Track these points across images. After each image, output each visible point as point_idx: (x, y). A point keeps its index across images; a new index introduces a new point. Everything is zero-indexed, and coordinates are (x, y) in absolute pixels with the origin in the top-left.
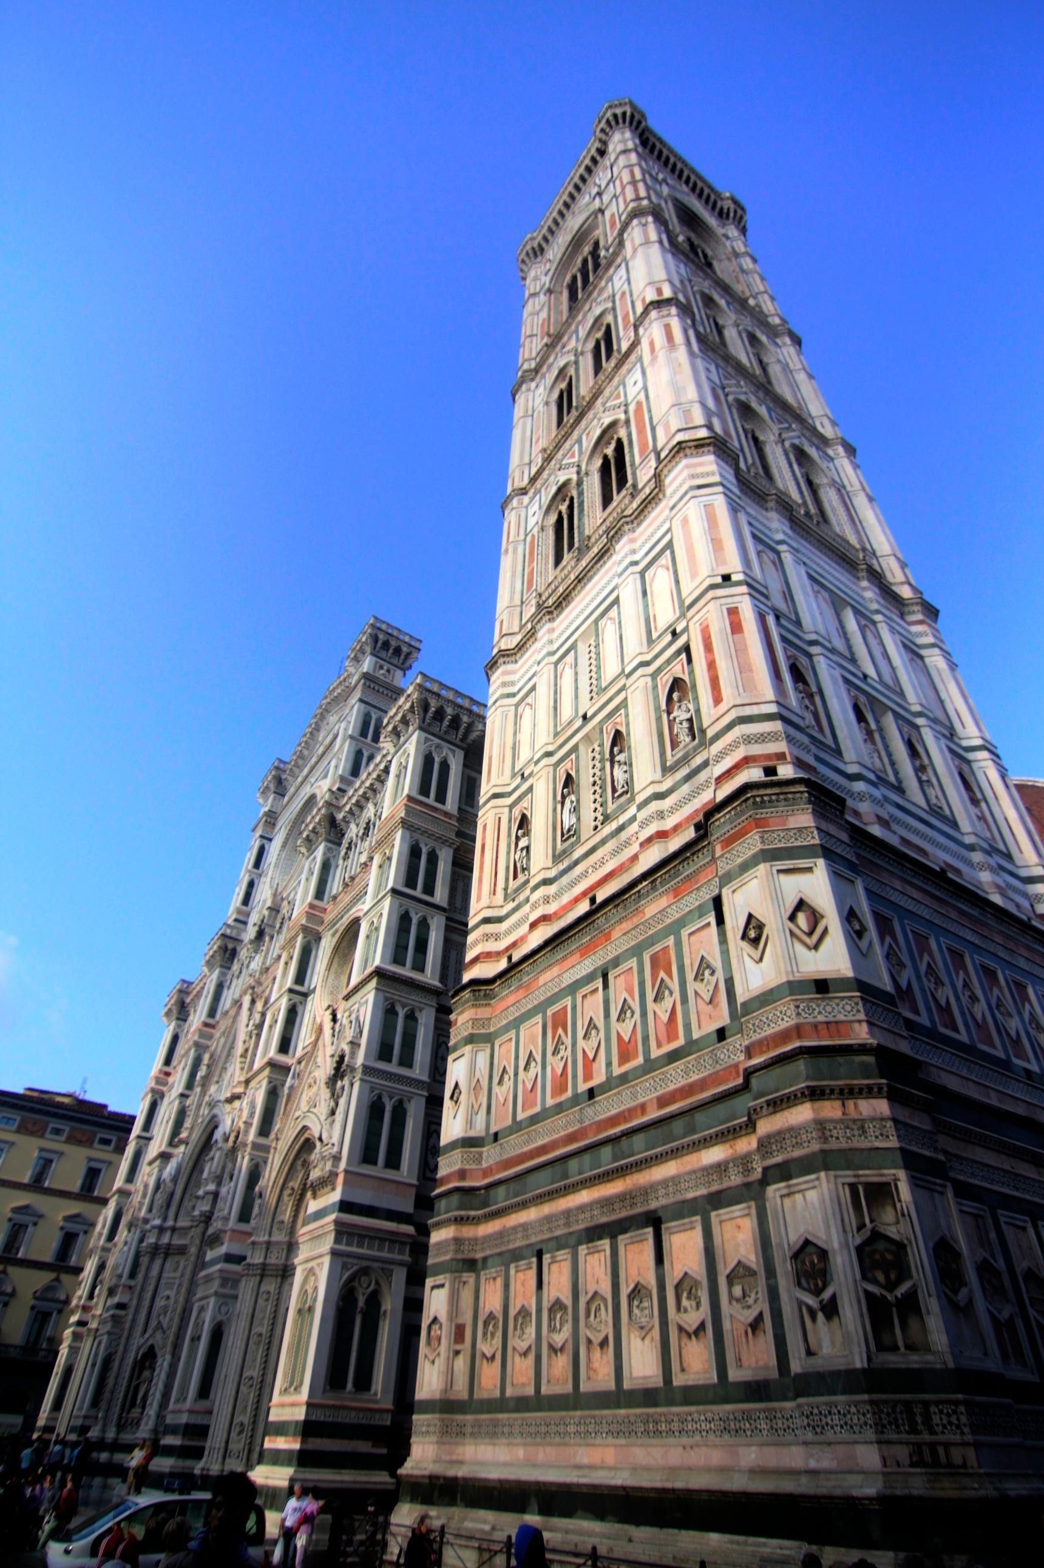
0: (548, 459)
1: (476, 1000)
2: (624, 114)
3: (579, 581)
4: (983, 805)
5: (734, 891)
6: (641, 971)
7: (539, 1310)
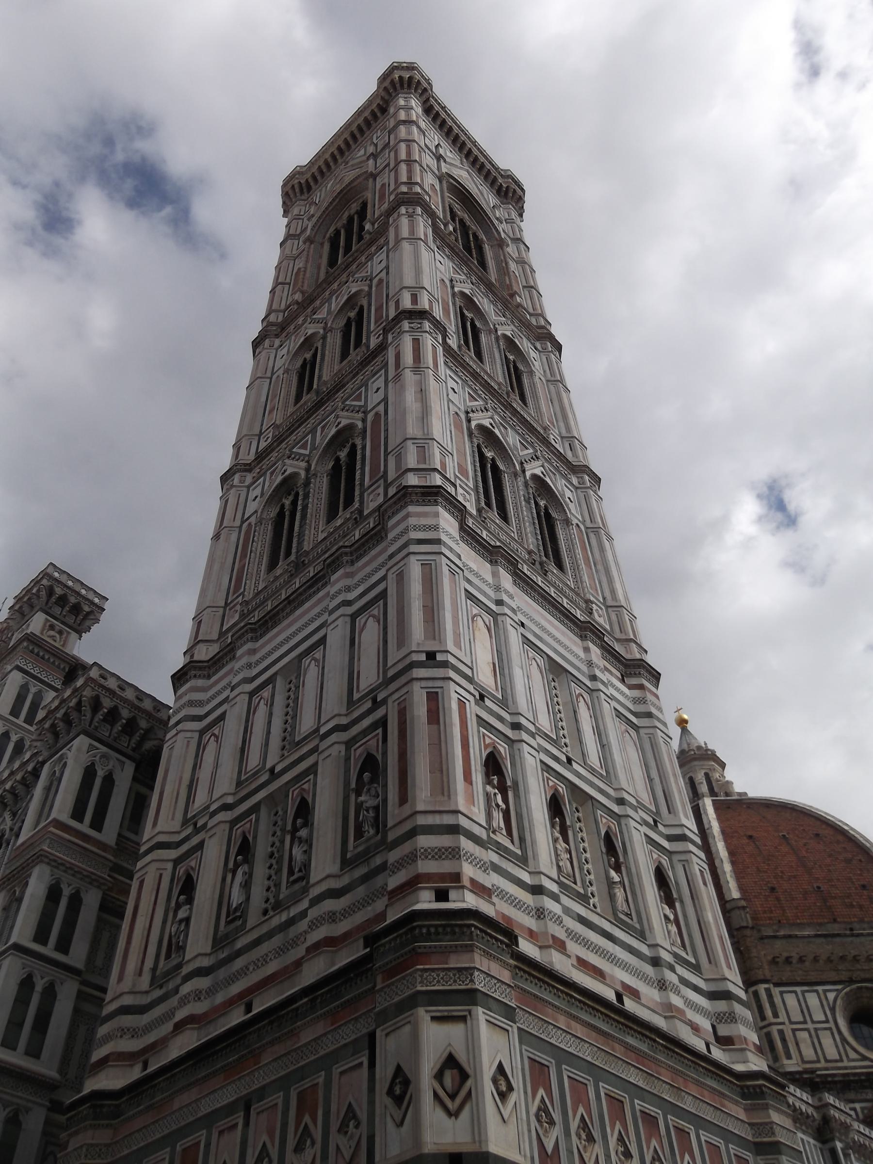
0: (279, 440)
2: (410, 78)
3: (289, 603)
4: (677, 905)
5: (387, 1035)
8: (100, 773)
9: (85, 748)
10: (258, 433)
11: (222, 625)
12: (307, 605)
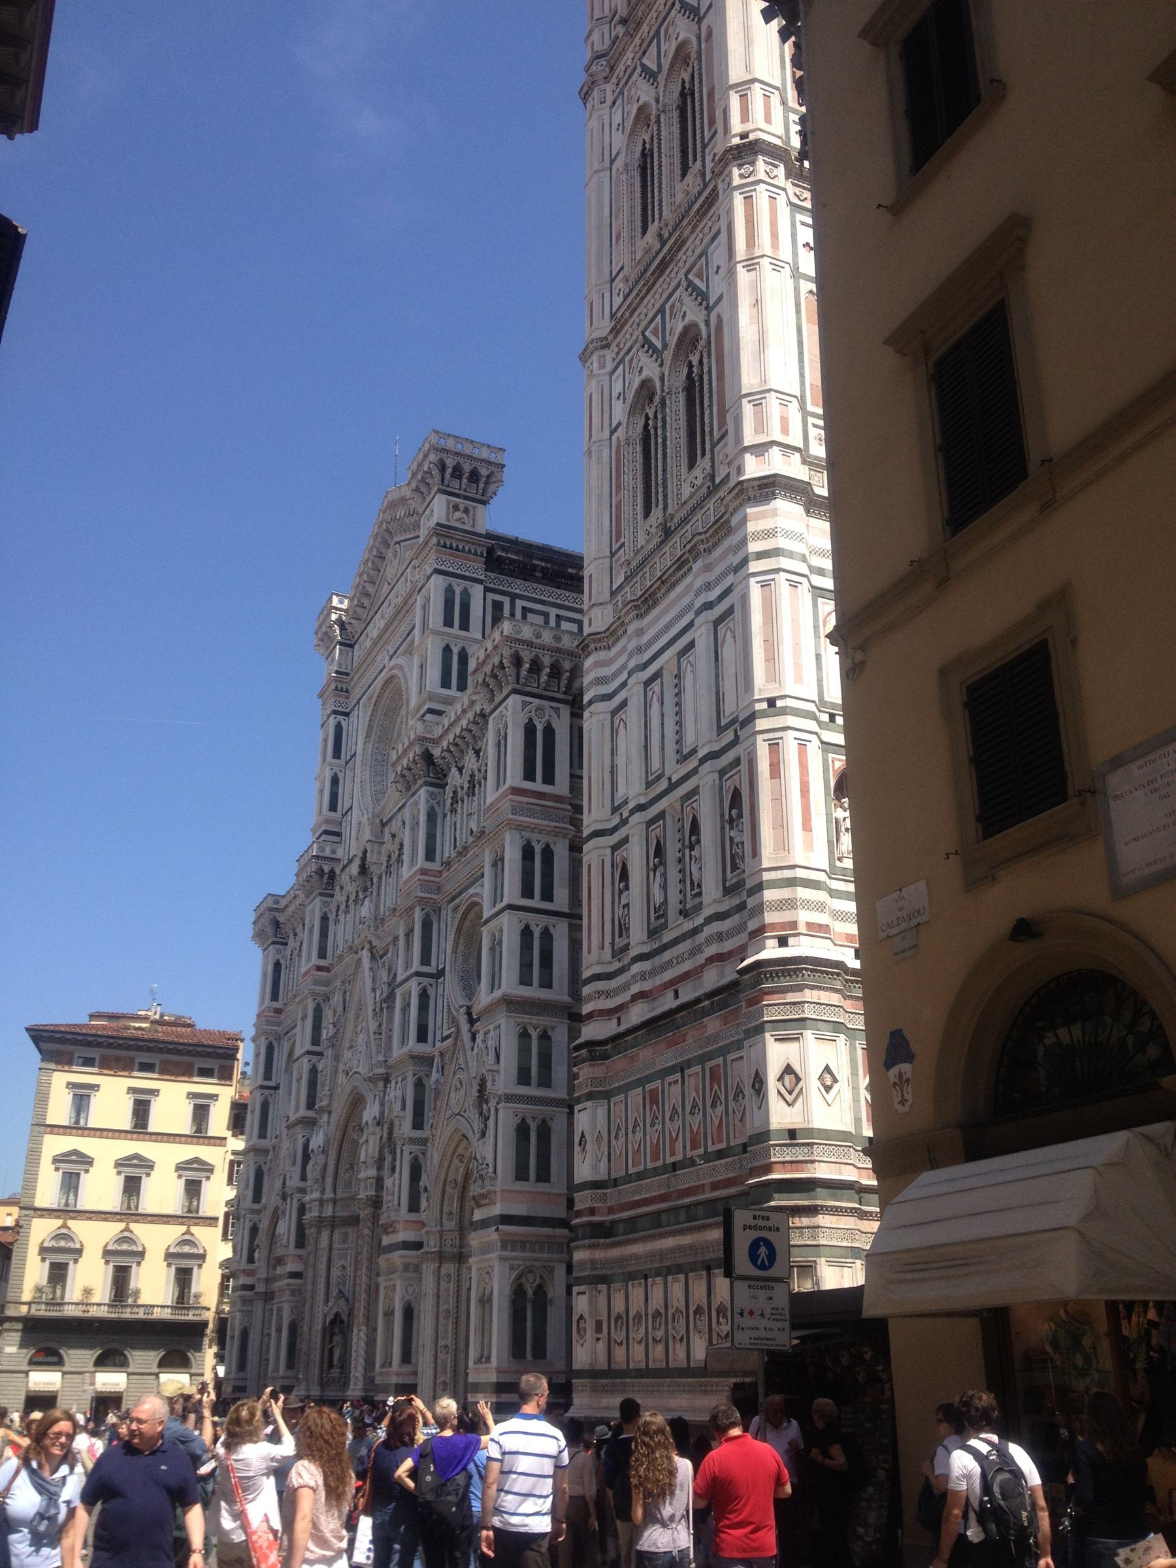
1: (593, 1059)
6: (704, 1079)
7: (646, 1315)
8: (540, 728)
9: (520, 708)
10: (608, 278)
11: (611, 582)
12: (679, 589)
